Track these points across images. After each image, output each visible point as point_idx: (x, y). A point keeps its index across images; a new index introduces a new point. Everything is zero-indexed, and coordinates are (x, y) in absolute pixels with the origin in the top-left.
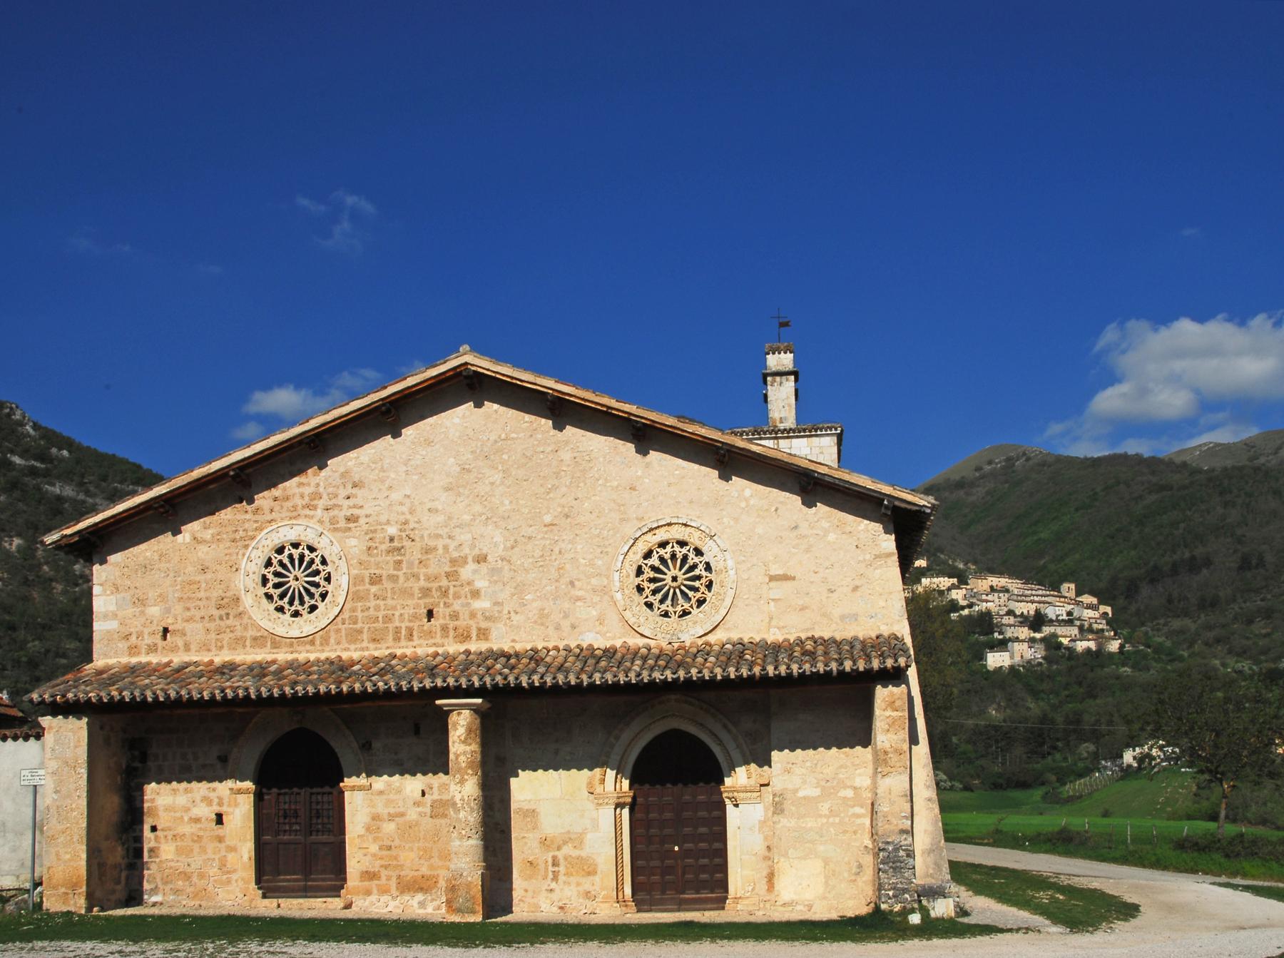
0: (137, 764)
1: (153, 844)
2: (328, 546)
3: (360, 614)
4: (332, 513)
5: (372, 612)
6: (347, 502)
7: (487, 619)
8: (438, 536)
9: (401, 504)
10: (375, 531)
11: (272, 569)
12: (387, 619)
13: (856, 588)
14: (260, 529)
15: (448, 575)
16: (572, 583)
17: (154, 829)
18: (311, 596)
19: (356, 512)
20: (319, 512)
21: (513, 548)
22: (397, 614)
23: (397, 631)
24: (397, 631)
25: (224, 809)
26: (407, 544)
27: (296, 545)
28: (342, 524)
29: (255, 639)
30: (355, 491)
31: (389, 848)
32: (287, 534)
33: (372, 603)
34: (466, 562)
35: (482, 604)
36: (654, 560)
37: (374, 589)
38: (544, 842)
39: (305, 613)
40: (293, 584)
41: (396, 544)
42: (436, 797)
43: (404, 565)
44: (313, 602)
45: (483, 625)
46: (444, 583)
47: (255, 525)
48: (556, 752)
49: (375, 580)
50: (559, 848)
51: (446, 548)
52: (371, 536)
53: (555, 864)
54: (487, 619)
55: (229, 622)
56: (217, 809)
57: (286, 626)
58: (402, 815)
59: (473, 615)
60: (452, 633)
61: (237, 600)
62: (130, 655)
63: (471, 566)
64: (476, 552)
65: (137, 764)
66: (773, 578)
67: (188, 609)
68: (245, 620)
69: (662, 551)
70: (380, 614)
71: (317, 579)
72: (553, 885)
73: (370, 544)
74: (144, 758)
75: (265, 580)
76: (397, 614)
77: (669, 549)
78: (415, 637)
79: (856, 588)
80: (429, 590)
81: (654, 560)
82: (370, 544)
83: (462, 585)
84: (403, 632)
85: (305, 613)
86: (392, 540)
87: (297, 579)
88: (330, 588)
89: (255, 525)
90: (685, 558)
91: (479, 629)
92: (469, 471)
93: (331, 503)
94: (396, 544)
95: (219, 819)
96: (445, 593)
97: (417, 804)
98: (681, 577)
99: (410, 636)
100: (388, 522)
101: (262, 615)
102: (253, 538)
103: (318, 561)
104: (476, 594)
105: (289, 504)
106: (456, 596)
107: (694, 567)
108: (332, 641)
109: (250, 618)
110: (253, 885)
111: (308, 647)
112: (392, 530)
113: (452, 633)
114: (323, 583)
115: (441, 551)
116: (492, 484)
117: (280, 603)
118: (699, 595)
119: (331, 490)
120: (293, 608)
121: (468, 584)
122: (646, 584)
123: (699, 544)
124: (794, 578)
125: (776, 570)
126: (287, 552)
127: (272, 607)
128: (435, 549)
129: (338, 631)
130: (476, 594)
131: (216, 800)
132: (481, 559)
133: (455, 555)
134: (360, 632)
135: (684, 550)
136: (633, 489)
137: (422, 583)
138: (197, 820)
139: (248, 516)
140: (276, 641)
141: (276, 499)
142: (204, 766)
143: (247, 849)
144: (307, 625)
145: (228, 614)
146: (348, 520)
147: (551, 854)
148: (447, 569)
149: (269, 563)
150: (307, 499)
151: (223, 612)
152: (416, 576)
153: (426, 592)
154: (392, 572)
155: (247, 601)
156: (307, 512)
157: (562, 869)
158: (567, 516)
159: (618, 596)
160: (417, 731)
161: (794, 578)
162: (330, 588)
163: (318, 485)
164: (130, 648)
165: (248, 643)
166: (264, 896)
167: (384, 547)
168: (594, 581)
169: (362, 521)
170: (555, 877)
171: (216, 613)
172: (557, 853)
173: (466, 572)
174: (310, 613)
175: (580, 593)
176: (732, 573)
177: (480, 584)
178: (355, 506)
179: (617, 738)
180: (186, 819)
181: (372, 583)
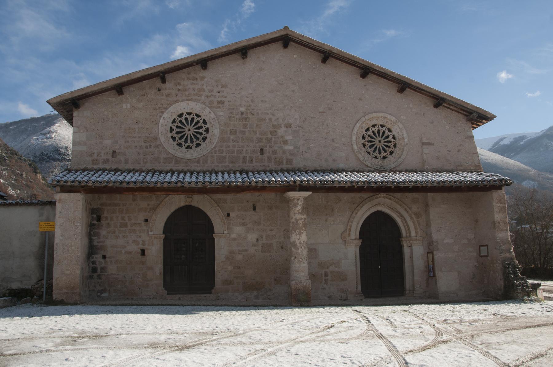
0: (95, 222)
1: (103, 265)
2: (207, 114)
3: (224, 149)
4: (210, 99)
5: (231, 148)
6: (218, 94)
7: (292, 154)
8: (266, 114)
9: (247, 97)
10: (233, 109)
11: (176, 124)
12: (239, 152)
13: (459, 151)
14: (170, 105)
15: (271, 132)
16: (333, 140)
17: (104, 257)
18: (198, 139)
19: (223, 99)
20: (203, 98)
21: (304, 121)
22: (244, 150)
23: (244, 158)
24: (244, 158)
25: (145, 247)
26: (250, 116)
27: (189, 114)
28: (215, 104)
29: (166, 159)
30: (223, 89)
31: (239, 268)
32: (183, 107)
33: (231, 144)
34: (281, 127)
35: (287, 147)
36: (370, 133)
37: (232, 137)
38: (321, 265)
39: (193, 147)
40: (187, 132)
41: (244, 116)
42: (264, 242)
43: (248, 126)
44: (198, 142)
45: (290, 157)
46: (269, 136)
47: (167, 102)
48: (326, 220)
49: (233, 132)
50: (328, 268)
51: (270, 119)
52: (231, 111)
53: (326, 275)
54: (292, 154)
55: (150, 150)
56: (141, 247)
57: (182, 153)
58: (246, 251)
59: (284, 152)
60: (273, 161)
61: (156, 139)
62: (93, 164)
63: (283, 129)
64: (286, 122)
65: (95, 222)
66: (423, 144)
67: (128, 142)
68: (160, 149)
69: (373, 129)
70: (236, 149)
71: (201, 131)
72: (325, 286)
73: (231, 115)
74: (99, 219)
75: (171, 130)
76: (244, 150)
77: (377, 128)
78: (254, 161)
79: (459, 151)
80: (261, 139)
81: (370, 133)
82: (231, 115)
83: (278, 138)
84: (248, 158)
85: (193, 147)
86: (242, 113)
87: (189, 131)
88: (208, 135)
89: (167, 102)
90: (384, 133)
91: (287, 159)
92: (282, 84)
93: (210, 94)
94: (244, 116)
95: (143, 252)
96: (269, 141)
97: (254, 245)
98: (377, 141)
99: (251, 161)
100: (240, 105)
101: (171, 148)
102: (166, 109)
103: (201, 122)
104: (286, 142)
105: (187, 93)
106: (276, 143)
107: (388, 137)
108: (209, 162)
109: (164, 148)
110: (161, 288)
111: (196, 164)
112: (242, 109)
113: (273, 161)
114: (204, 133)
115: (268, 121)
116: (294, 91)
117: (180, 141)
118: (390, 150)
119: (209, 88)
120: (187, 144)
121: (282, 137)
122: (366, 143)
123: (390, 127)
124: (433, 144)
125: (425, 140)
126: (184, 117)
127: (175, 143)
128: (265, 120)
129: (213, 157)
130: (286, 142)
131: (141, 242)
132: (288, 126)
133: (275, 123)
134: (225, 158)
135: (384, 129)
136: (360, 99)
137: (258, 135)
138: (130, 253)
139: (163, 98)
140: (178, 161)
141: (179, 90)
142: (135, 224)
143: (159, 268)
144: (194, 153)
145: (150, 146)
146: (219, 103)
147: (324, 271)
148: (271, 129)
149: (174, 121)
150: (196, 91)
151: (147, 144)
152: (255, 132)
153: (260, 140)
154: (242, 129)
155: (162, 139)
156: (197, 97)
157: (329, 278)
158: (330, 109)
159: (355, 147)
160: (254, 209)
161: (433, 144)
162: (208, 135)
163: (203, 85)
164: (93, 160)
165: (161, 161)
166: (168, 294)
167: (237, 117)
168: (343, 140)
169: (226, 104)
170: (326, 282)
171: (144, 145)
172: (327, 270)
173: (281, 131)
174: (196, 147)
175: (337, 145)
176: (406, 140)
177: (288, 138)
178: (222, 96)
179: (356, 214)
180: (123, 252)
181: (231, 134)
